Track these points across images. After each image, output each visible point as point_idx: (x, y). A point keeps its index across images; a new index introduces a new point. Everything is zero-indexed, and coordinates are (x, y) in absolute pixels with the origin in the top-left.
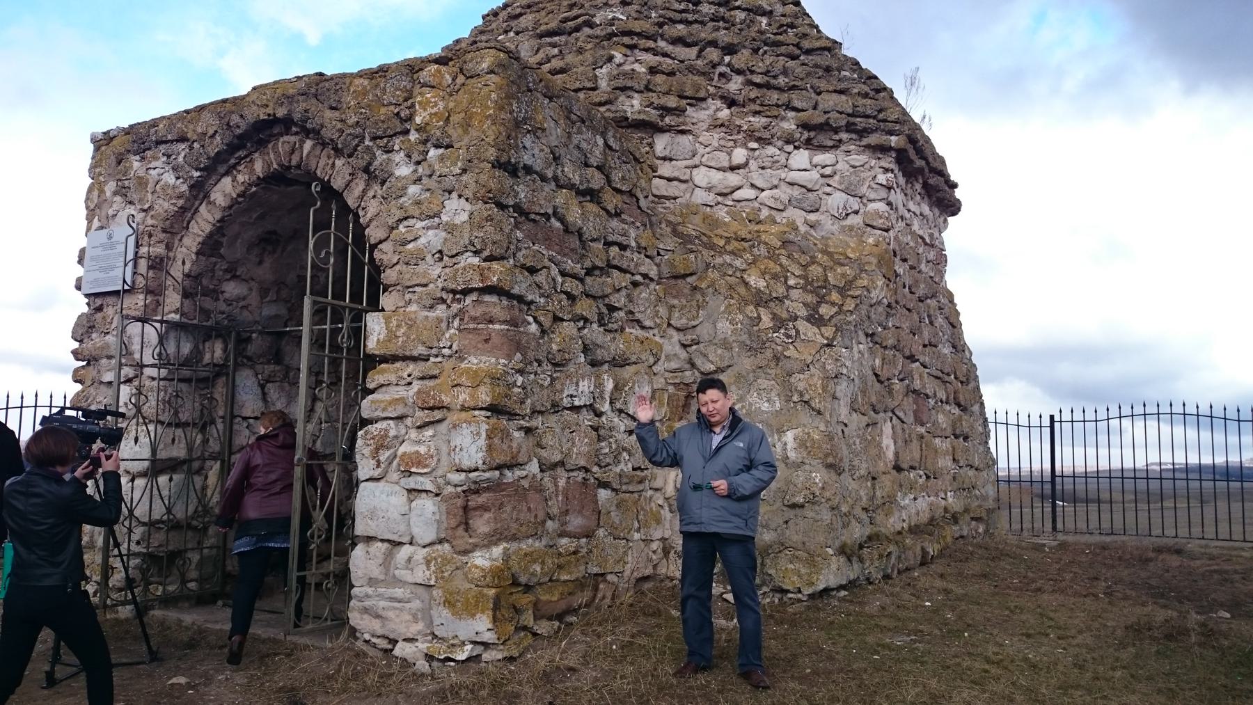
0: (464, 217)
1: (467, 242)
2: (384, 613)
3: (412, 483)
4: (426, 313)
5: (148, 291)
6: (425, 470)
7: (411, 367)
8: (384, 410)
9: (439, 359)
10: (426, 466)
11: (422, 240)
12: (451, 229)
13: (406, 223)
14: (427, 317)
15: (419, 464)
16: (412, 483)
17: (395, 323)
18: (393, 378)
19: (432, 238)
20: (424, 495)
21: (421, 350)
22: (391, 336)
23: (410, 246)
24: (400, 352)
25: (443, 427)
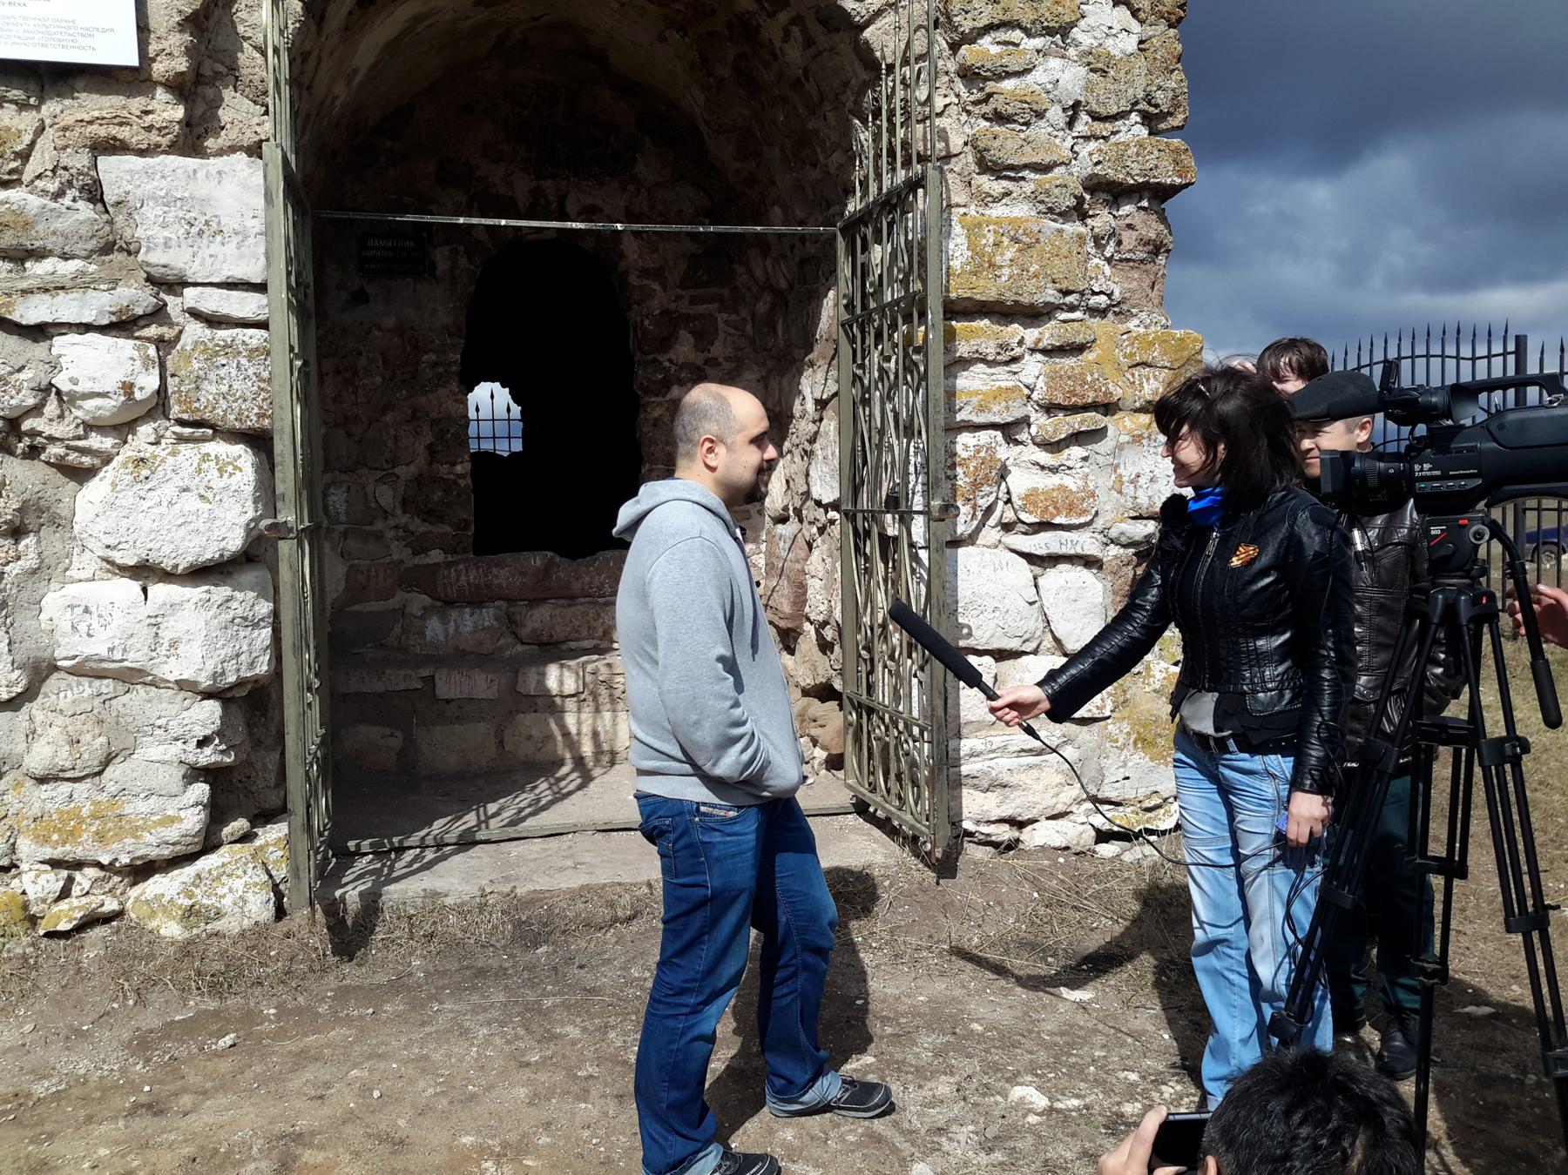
0: (1130, 44)
1: (1141, 95)
2: (1013, 780)
3: (1042, 543)
4: (1058, 226)
5: (180, 88)
6: (1082, 520)
7: (1015, 331)
8: (982, 409)
9: (1078, 315)
10: (1085, 511)
11: (1038, 77)
12: (1098, 65)
13: (1002, 35)
14: (1060, 231)
15: (1070, 509)
16: (1042, 543)
17: (991, 238)
18: (990, 350)
19: (1061, 75)
20: (1063, 567)
21: (1050, 295)
22: (984, 264)
23: (1008, 85)
24: (1009, 297)
25: (1105, 446)
